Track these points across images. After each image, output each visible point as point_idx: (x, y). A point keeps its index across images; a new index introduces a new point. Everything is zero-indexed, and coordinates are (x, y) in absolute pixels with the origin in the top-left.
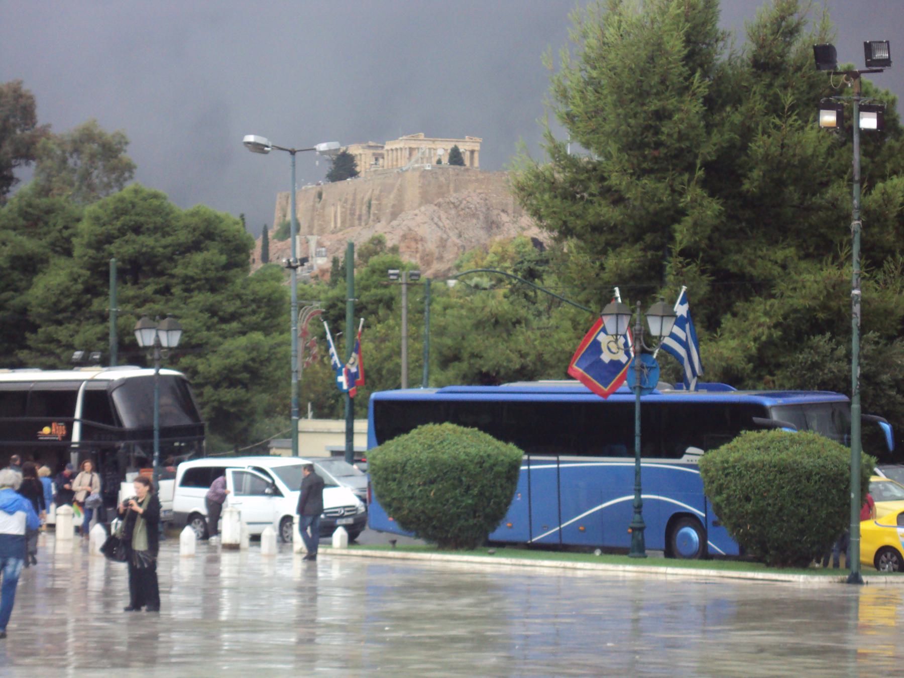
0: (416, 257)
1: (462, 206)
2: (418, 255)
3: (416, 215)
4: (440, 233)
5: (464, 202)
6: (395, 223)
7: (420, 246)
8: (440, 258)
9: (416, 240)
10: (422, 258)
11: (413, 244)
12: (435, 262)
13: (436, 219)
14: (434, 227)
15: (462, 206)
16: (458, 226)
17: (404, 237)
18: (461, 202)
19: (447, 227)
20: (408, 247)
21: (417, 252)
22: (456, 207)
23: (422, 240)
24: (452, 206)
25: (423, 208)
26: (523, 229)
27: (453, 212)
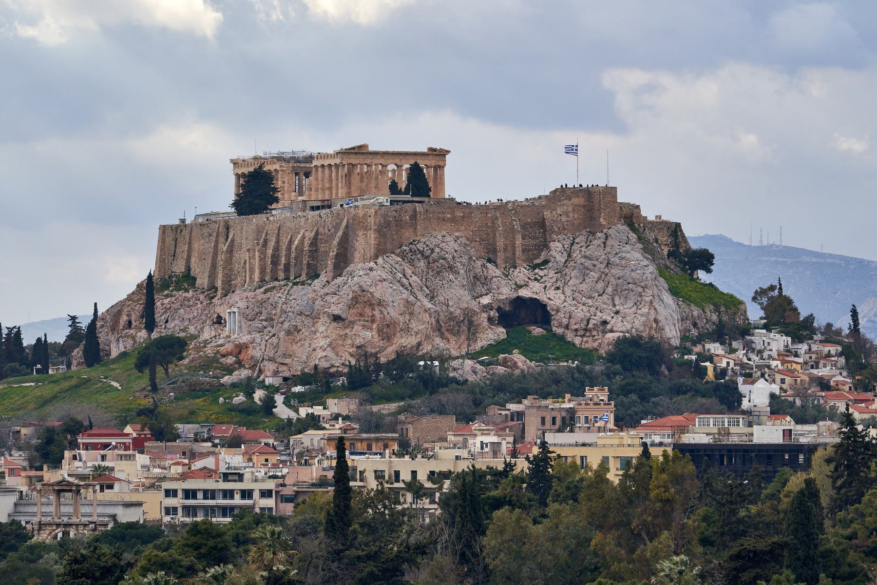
0: (371, 329)
1: (434, 255)
2: (375, 326)
3: (371, 269)
4: (406, 294)
5: (437, 250)
6: (339, 280)
7: (377, 313)
8: (407, 330)
9: (372, 306)
10: (380, 331)
11: (368, 311)
12: (398, 335)
13: (399, 275)
14: (397, 286)
16: (429, 284)
18: (432, 252)
19: (414, 284)
20: (361, 315)
21: (373, 321)
23: (380, 303)
24: (419, 256)
25: (380, 260)
27: (422, 264)
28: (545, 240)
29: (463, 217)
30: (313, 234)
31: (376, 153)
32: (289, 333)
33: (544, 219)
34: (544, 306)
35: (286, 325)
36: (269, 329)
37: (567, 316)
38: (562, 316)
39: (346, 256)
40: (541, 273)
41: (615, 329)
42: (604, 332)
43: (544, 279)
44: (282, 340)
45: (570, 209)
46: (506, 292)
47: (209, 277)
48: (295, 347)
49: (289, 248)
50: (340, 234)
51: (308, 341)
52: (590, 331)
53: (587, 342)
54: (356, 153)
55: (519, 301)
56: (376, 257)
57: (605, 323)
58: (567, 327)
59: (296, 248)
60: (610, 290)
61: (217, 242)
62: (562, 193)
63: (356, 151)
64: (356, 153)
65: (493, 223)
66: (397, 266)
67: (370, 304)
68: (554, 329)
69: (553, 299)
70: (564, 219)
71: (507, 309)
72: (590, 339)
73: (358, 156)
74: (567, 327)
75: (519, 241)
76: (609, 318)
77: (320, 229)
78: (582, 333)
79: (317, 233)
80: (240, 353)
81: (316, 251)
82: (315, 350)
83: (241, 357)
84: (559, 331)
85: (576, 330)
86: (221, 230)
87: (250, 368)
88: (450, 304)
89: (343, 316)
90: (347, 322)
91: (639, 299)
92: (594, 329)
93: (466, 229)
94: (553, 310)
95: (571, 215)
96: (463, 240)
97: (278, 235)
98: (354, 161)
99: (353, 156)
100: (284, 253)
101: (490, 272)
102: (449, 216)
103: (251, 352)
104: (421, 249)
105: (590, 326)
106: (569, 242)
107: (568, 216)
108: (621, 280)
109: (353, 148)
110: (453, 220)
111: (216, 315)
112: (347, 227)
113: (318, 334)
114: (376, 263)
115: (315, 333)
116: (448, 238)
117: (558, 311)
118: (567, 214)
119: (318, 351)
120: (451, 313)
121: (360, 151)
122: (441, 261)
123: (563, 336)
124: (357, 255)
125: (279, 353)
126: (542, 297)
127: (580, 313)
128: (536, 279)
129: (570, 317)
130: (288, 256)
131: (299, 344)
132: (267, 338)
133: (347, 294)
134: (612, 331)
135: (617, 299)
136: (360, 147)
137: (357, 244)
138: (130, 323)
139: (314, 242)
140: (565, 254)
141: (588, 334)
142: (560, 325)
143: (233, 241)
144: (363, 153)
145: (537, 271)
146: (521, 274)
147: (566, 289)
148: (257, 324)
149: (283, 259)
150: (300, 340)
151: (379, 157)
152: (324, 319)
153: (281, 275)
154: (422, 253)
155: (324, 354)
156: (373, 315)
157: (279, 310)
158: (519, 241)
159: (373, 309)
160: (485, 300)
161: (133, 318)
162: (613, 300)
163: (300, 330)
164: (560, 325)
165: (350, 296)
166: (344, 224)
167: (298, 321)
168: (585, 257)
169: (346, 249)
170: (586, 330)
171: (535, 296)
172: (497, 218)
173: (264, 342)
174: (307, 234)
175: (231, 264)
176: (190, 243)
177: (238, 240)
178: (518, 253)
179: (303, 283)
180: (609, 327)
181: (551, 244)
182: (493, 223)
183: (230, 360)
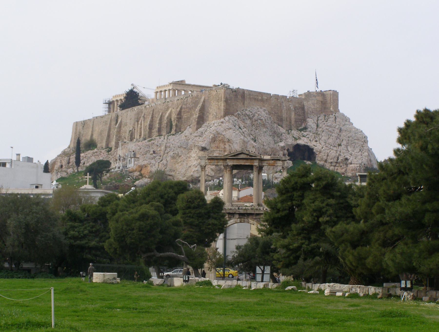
1: (256, 117)
3: (222, 122)
5: (257, 115)
6: (201, 130)
7: (227, 146)
11: (222, 145)
15: (256, 117)
16: (253, 133)
17: (214, 140)
20: (217, 147)
22: (250, 119)
23: (229, 141)
24: (247, 117)
25: (227, 118)
26: (296, 139)
27: (248, 122)
28: (305, 117)
29: (267, 100)
30: (179, 109)
31: (189, 85)
32: (173, 158)
33: (304, 106)
34: (313, 149)
35: (171, 154)
36: (158, 157)
37: (326, 155)
38: (323, 155)
39: (203, 118)
40: (305, 134)
41: (353, 162)
42: (347, 164)
43: (307, 136)
44: (169, 162)
45: (315, 102)
46: (291, 141)
47: (106, 142)
48: (177, 165)
49: (161, 119)
50: (200, 105)
51: (185, 162)
52: (339, 163)
53: (337, 169)
54: (180, 84)
55: (297, 147)
56: (225, 116)
57: (347, 159)
58: (326, 161)
59: (167, 118)
60: (344, 142)
61: (110, 124)
62: (308, 95)
63: (180, 83)
64: (180, 84)
65: (281, 104)
66: (236, 122)
67: (223, 142)
68: (318, 162)
69: (317, 146)
70: (313, 107)
71: (291, 150)
72: (339, 168)
73: (181, 85)
74: (326, 161)
75: (293, 116)
76: (348, 157)
77: (184, 106)
78: (334, 164)
79: (181, 109)
80: (141, 170)
81: (180, 118)
82: (190, 167)
83: (142, 172)
84: (321, 163)
85: (331, 163)
86: (112, 118)
87: (149, 178)
88: (265, 144)
89: (208, 148)
90: (209, 151)
91: (362, 148)
92: (341, 162)
93: (268, 106)
94: (317, 151)
95: (316, 105)
96: (267, 111)
97: (153, 114)
98: (179, 88)
99: (178, 85)
100: (158, 122)
101: (281, 130)
102: (260, 98)
103: (149, 168)
104: (248, 114)
105: (340, 160)
106: (316, 118)
107: (314, 106)
108: (351, 138)
109: (178, 82)
110: (262, 100)
111: (118, 156)
112: (204, 101)
113: (192, 158)
114: (225, 119)
115: (190, 158)
116: (260, 110)
117: (320, 152)
118: (314, 104)
119: (192, 167)
120: (266, 150)
121: (181, 83)
122: (259, 121)
123: (323, 166)
124: (211, 117)
125: (168, 169)
126: (311, 144)
127: (333, 154)
128: (303, 136)
129: (328, 156)
130: (160, 123)
131: (180, 164)
132: (159, 161)
133: (208, 135)
134: (351, 164)
135: (349, 147)
136: (182, 81)
137: (211, 111)
138: (62, 166)
139: (180, 113)
140: (316, 125)
141: (338, 165)
142: (322, 160)
143: (121, 122)
144: (183, 84)
145: (302, 132)
146: (295, 133)
147: (321, 141)
148: (148, 155)
149: (157, 126)
150: (181, 162)
151: (190, 87)
152: (196, 150)
153: (156, 134)
154: (248, 116)
155: (196, 169)
156: (225, 148)
157: (163, 148)
158: (293, 116)
159: (225, 144)
160: (282, 144)
161: (63, 164)
162: (347, 148)
163: (180, 156)
164: (322, 160)
165: (211, 137)
166: (202, 100)
167: (179, 150)
168: (328, 126)
169: (203, 114)
170: (337, 163)
171: (307, 144)
172: (282, 102)
173: (157, 163)
174: (173, 110)
175: (120, 134)
176: (93, 128)
177: (124, 121)
178: (293, 122)
179: (173, 135)
180: (349, 161)
181: (308, 119)
182: (281, 104)
183: (137, 174)
